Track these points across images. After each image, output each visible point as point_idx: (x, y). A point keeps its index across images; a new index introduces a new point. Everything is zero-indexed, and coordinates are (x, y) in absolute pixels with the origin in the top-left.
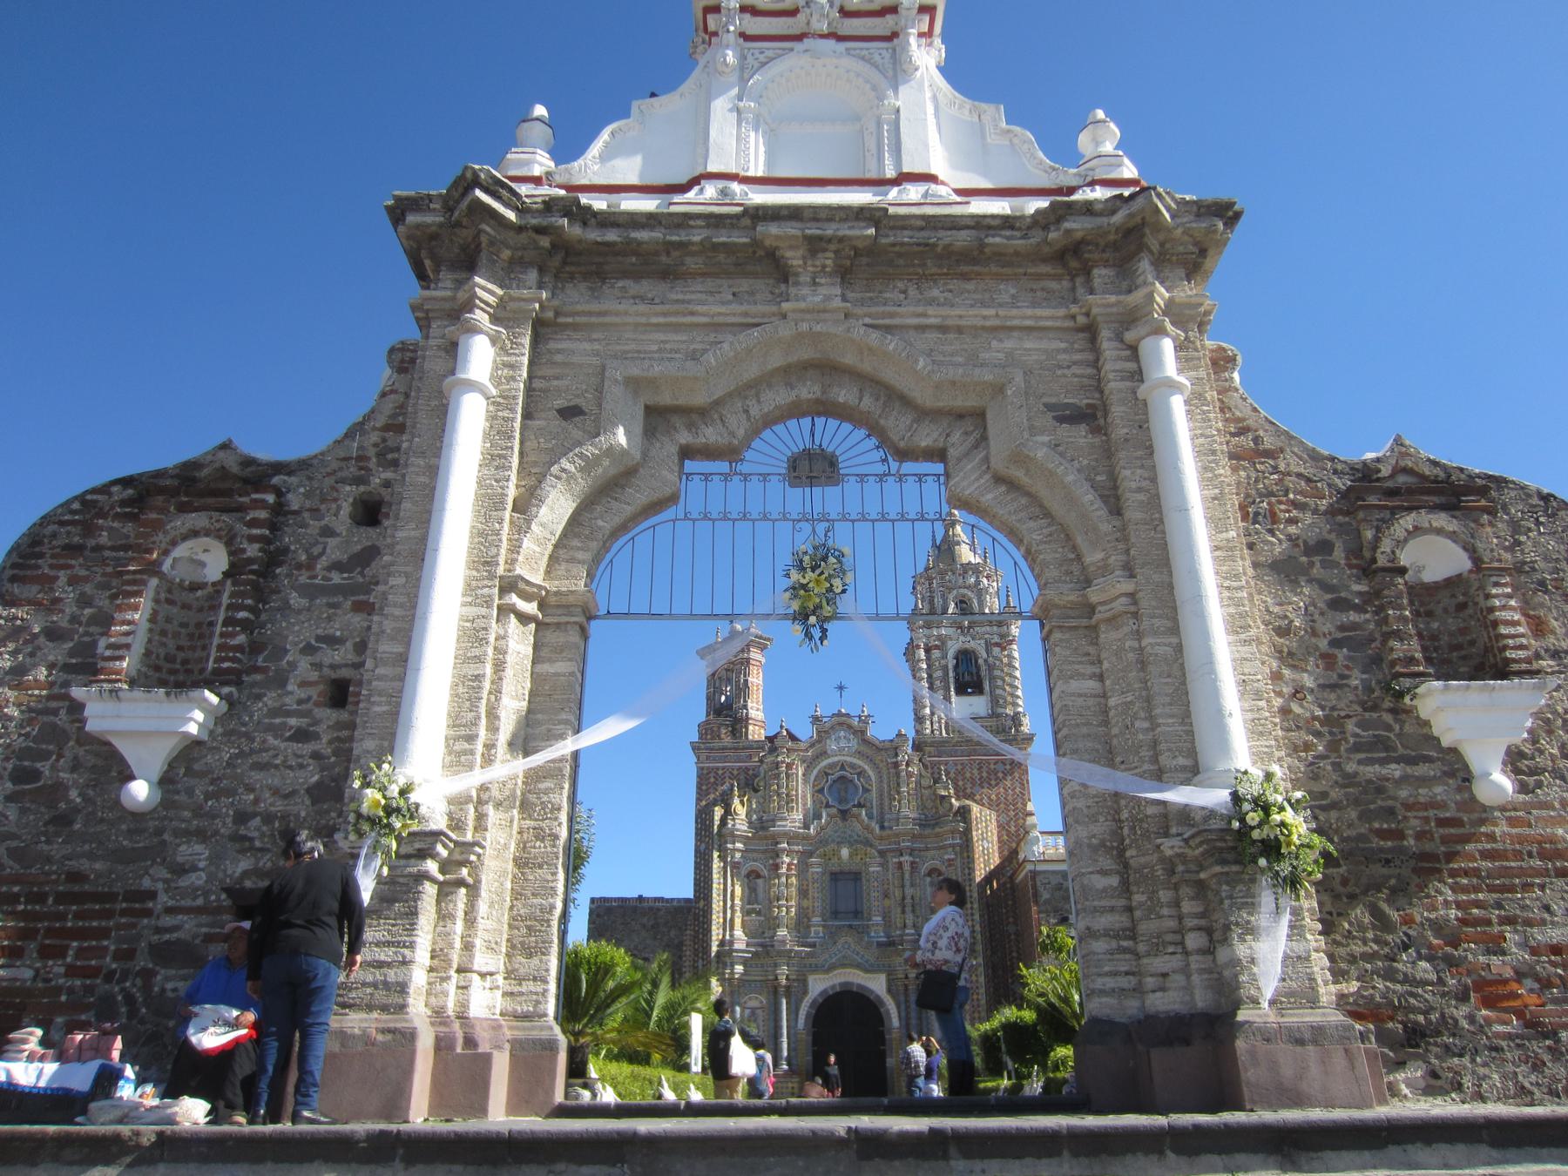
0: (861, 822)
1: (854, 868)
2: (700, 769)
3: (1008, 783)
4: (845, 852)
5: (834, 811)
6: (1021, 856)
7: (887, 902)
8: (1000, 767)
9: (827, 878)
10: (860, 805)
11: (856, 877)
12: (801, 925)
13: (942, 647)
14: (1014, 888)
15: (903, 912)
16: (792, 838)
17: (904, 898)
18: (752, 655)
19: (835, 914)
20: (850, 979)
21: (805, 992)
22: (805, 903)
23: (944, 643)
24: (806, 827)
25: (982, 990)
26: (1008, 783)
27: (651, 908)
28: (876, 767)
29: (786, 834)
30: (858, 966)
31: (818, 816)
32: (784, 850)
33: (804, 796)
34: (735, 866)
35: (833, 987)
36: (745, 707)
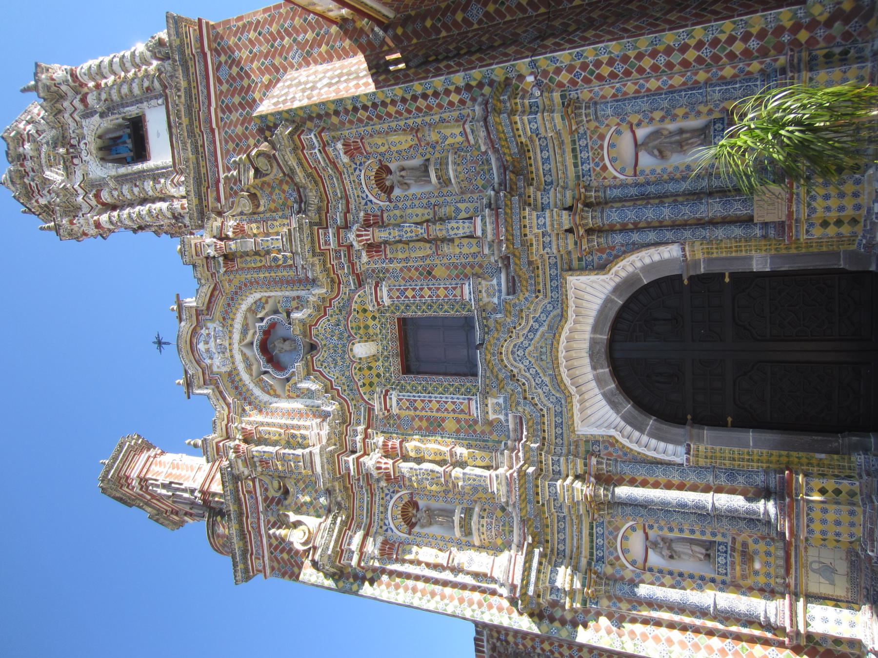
1: (393, 331)
3: (245, 54)
4: (362, 350)
8: (224, 72)
9: (410, 380)
12: (486, 439)
13: (95, 187)
14: (405, 21)
16: (342, 444)
18: (134, 474)
20: (586, 345)
21: (611, 442)
22: (450, 425)
24: (325, 416)
25: (589, 52)
29: (331, 459)
30: (555, 330)
31: (310, 394)
32: (358, 464)
33: (289, 414)
34: (390, 549)
35: (599, 380)
36: (192, 491)
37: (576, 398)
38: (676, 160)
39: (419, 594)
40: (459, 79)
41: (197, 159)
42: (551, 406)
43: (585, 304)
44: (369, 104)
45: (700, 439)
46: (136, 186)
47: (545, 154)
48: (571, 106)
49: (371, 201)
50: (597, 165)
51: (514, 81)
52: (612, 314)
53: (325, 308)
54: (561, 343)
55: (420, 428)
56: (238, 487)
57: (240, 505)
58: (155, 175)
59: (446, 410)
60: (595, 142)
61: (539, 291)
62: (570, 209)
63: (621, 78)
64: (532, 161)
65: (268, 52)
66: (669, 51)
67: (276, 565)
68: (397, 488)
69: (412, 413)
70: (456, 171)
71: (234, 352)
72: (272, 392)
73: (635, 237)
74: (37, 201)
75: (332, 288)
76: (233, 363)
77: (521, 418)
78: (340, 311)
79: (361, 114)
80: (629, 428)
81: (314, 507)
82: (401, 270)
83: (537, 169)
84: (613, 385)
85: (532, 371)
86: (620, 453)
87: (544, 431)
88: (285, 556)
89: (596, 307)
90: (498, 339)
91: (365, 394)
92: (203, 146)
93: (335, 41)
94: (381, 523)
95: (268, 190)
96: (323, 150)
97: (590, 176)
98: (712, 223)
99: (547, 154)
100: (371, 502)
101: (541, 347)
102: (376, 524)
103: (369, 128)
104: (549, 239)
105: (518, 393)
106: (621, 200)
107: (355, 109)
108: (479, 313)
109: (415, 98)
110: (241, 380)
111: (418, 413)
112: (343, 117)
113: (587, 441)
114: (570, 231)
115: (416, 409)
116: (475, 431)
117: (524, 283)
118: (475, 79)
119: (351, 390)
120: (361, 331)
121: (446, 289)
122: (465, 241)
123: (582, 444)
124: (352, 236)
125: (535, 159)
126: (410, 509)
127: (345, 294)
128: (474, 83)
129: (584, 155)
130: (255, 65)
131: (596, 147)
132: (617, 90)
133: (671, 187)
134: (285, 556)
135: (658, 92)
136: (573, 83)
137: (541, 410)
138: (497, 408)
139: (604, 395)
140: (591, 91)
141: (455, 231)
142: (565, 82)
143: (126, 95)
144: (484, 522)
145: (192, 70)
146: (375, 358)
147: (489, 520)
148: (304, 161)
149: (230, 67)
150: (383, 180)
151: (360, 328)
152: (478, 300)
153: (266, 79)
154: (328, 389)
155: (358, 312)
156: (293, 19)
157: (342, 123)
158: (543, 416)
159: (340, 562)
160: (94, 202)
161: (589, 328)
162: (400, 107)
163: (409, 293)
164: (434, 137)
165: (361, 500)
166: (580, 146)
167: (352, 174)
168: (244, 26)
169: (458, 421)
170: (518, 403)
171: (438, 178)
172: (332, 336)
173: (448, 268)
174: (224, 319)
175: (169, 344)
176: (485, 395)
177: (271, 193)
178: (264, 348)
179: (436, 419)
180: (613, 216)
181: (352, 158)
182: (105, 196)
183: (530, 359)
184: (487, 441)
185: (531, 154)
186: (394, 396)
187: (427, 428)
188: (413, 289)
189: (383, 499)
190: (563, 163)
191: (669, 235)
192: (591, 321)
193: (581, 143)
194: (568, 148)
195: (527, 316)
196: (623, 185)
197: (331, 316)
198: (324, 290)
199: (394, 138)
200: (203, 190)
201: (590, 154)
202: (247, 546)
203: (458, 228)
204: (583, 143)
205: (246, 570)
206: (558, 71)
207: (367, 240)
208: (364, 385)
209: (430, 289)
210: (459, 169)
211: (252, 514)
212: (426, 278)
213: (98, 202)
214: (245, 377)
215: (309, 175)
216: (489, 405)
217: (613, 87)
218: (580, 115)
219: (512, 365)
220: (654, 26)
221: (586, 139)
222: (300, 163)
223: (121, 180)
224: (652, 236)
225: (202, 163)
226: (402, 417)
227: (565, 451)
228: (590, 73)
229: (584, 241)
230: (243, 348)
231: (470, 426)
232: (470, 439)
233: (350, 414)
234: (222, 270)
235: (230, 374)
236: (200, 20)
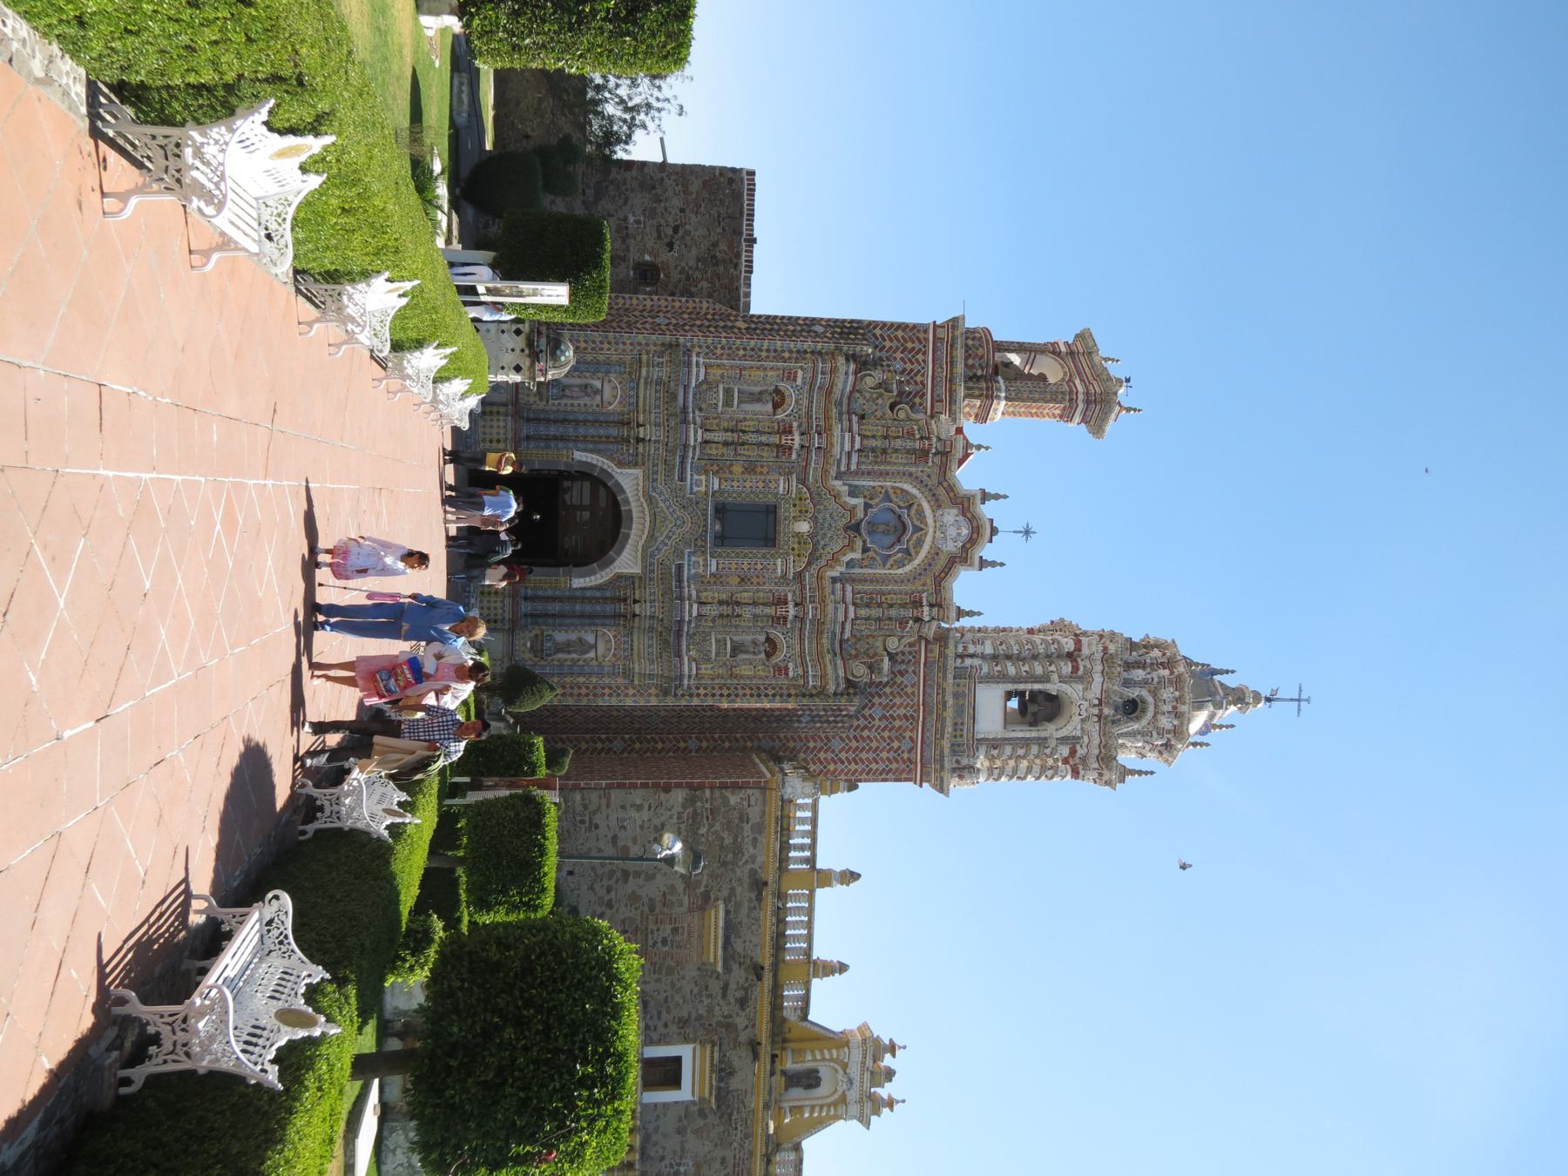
0: (842, 551)
1: (781, 538)
2: (923, 329)
4: (804, 527)
5: (860, 514)
6: (787, 767)
8: (906, 745)
9: (771, 499)
10: (865, 550)
13: (1074, 677)
15: (721, 603)
17: (738, 604)
19: (721, 510)
21: (620, 464)
23: (1080, 679)
25: (614, 702)
26: (884, 755)
27: (738, 255)
28: (916, 576)
30: (652, 536)
35: (627, 502)
38: (573, 636)
40: (696, 702)
45: (566, 464)
48: (628, 674)
52: (617, 545)
58: (1003, 678)
62: (635, 615)
66: (572, 695)
67: (921, 336)
73: (598, 594)
79: (770, 692)
88: (909, 345)
95: (871, 652)
98: (554, 599)
100: (810, 407)
106: (606, 617)
107: (774, 695)
113: (636, 465)
114: (635, 602)
124: (792, 611)
130: (874, 744)
133: (577, 621)
134: (909, 345)
135: (579, 675)
150: (772, 646)
153: (866, 733)
154: (837, 497)
160: (1081, 665)
162: (741, 692)
163: (759, 567)
165: (818, 407)
176: (706, 493)
180: (609, 608)
182: (1067, 668)
191: (578, 594)
196: (604, 625)
205: (953, 327)
214: (925, 505)
220: (579, 710)
223: (1045, 679)
224: (588, 594)
228: (615, 691)
235: (939, 507)
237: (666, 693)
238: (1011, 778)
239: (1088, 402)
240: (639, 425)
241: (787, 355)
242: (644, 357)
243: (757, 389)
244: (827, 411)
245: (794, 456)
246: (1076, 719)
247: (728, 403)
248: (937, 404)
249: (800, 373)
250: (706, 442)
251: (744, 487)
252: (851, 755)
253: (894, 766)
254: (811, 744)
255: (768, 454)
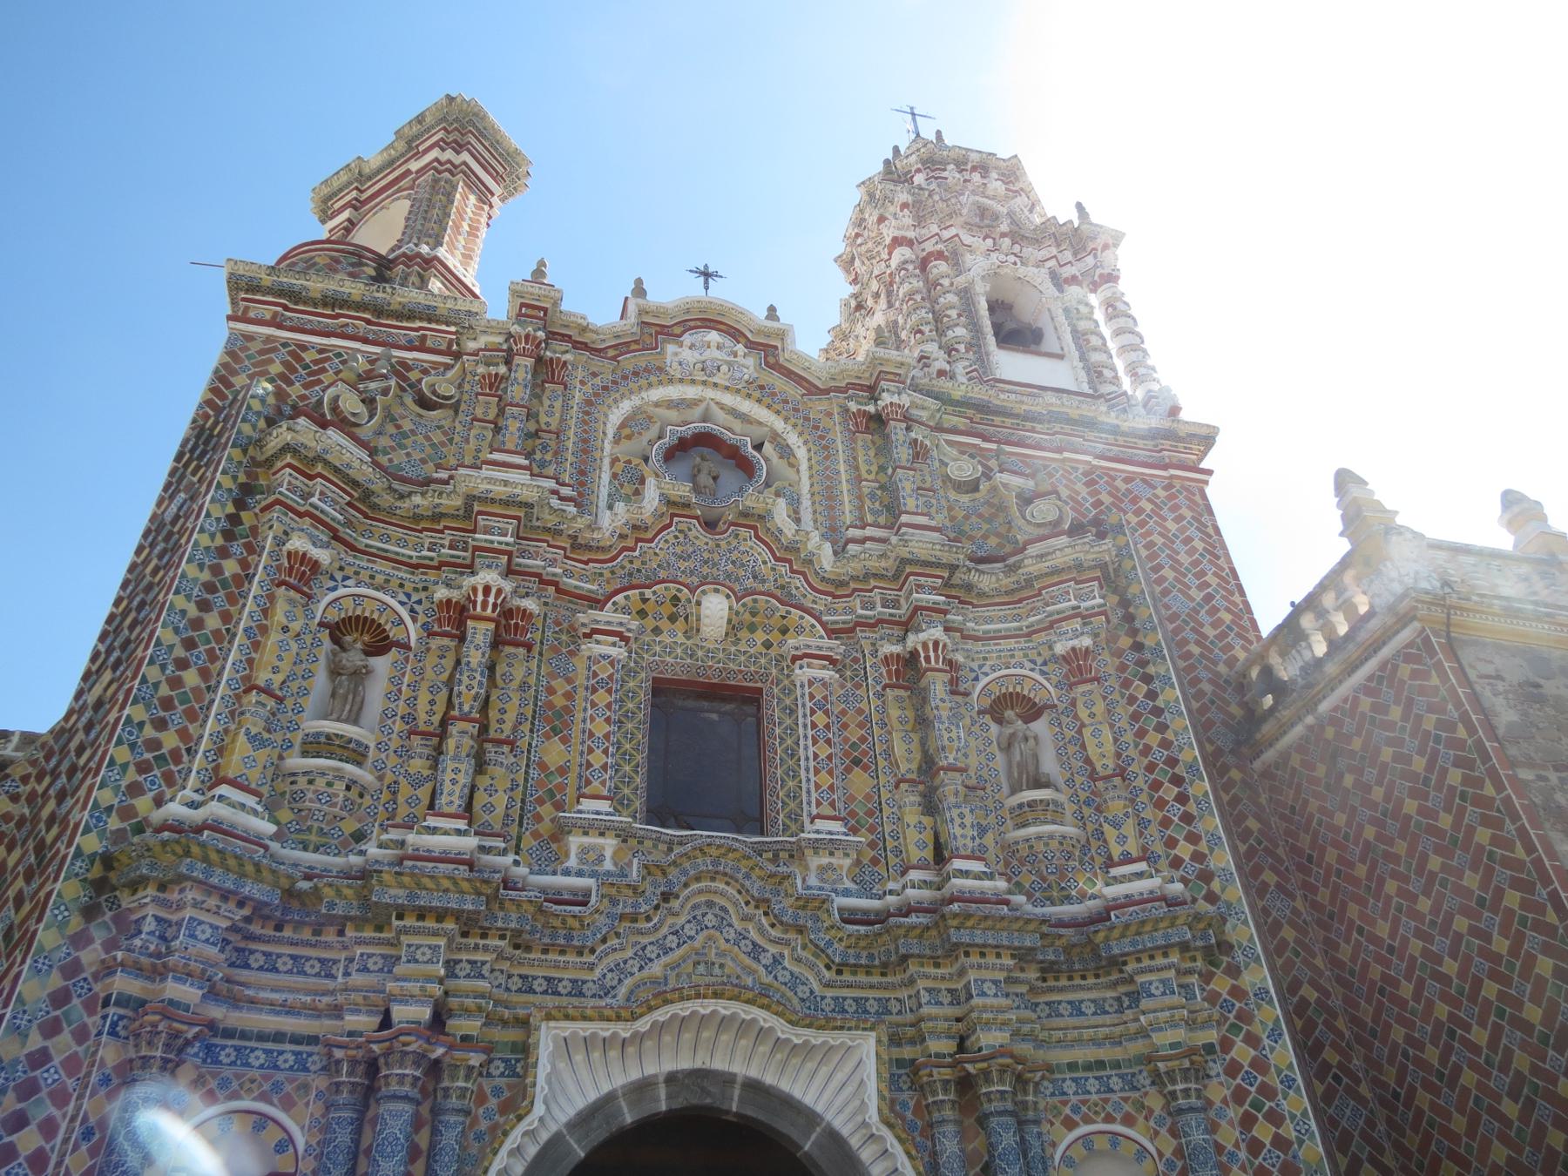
4: (715, 609)
7: (860, 781)
11: (744, 699)
13: (954, 258)
20: (719, 1064)
21: (516, 1103)
25: (1297, 1103)
26: (1172, 527)
35: (642, 1088)
37: (624, 1030)
39: (193, 612)
40: (1223, 859)
41: (1017, 416)
42: (597, 973)
43: (810, 1066)
44: (1160, 703)
46: (959, 315)
47: (1089, 1009)
48: (1196, 1062)
49: (976, 679)
50: (1076, 1109)
51: (1225, 959)
52: (783, 1126)
53: (789, 561)
54: (747, 1007)
55: (551, 691)
56: (438, 322)
57: (399, 316)
59: (591, 751)
60: (1117, 1107)
61: (839, 972)
63: (1252, 1164)
64: (1077, 981)
65: (1177, 561)
67: (255, 347)
68: (421, 618)
69: (581, 680)
70: (1051, 837)
71: (700, 388)
72: (627, 431)
74: (918, 171)
75: (823, 579)
76: (681, 381)
77: (584, 904)
78: (782, 587)
80: (532, 1151)
81: (392, 448)
82: (860, 711)
83: (1061, 990)
84: (629, 1119)
85: (672, 941)
86: (484, 1125)
87: (545, 951)
89: (797, 1093)
90: (747, 876)
91: (627, 598)
92: (1033, 430)
93: (1206, 668)
94: (349, 571)
96: (1076, 613)
97: (1053, 1094)
99: (1089, 1012)
101: (722, 966)
102: (351, 560)
103: (1116, 696)
104: (946, 1001)
105: (635, 905)
107: (1148, 679)
108: (788, 846)
109: (1177, 780)
110: (650, 385)
111: (581, 693)
112: (1132, 656)
115: (594, 690)
116: (541, 802)
117: (863, 943)
118: (1223, 890)
119: (631, 575)
120: (747, 616)
121: (831, 787)
122: (928, 837)
123: (513, 1035)
125: (1082, 988)
126: (366, 638)
127: (815, 602)
128: (1216, 885)
129: (1092, 1085)
130: (1160, 541)
131: (1109, 1108)
132: (1232, 1155)
136: (1233, 1069)
137: (592, 951)
138: (592, 856)
139: (610, 1098)
140: (1225, 1101)
141: (958, 821)
142: (1233, 1054)
143: (1088, 341)
144: (340, 787)
145: (1141, 443)
146: (693, 630)
147: (340, 799)
148: (1056, 579)
149: (1149, 500)
150: (1013, 706)
151: (754, 614)
152: (816, 846)
155: (784, 617)
156: (1228, 610)
157: (1118, 653)
158: (580, 954)
159: (289, 465)
161: (753, 1073)
162: (1160, 755)
164: (1116, 807)
166: (1109, 1077)
167: (1026, 656)
168: (1210, 537)
169: (562, 771)
170: (614, 902)
171: (1032, 804)
172: (733, 562)
173: (868, 797)
174: (762, 387)
175: (707, 288)
176: (624, 835)
177: (980, 516)
178: (705, 440)
179: (567, 725)
181: (1065, 659)
183: (701, 938)
184: (521, 825)
185: (1091, 981)
186: (618, 652)
187: (550, 705)
188: (827, 726)
189: (401, 585)
190: (1079, 1041)
192: (769, 1079)
193: (1115, 1079)
194: (1105, 1053)
195: (787, 943)
197: (773, 569)
198: (828, 568)
199: (1108, 736)
200: (970, 412)
201: (1095, 1097)
202: (305, 303)
203: (963, 826)
204: (1116, 1083)
205: (253, 287)
206: (1252, 1040)
207: (928, 659)
208: (645, 601)
209: (830, 757)
210: (1054, 844)
211: (375, 333)
212: (847, 754)
213: (930, 254)
215: (1029, 583)
216: (601, 840)
217: (1237, 1145)
218: (1186, 1079)
219: (687, 899)
221: (1122, 1090)
222: (1056, 571)
223: (966, 294)
225: (1009, 422)
226: (574, 660)
227: (500, 994)
228: (1256, 1103)
229: (946, 1073)
230: (703, 406)
231: (551, 794)
232: (525, 788)
233: (586, 563)
234: (853, 406)
236: (1210, 472)
237: (1218, 952)
238: (1144, 351)
239: (459, 147)
240: (386, 1023)
241: (230, 567)
242: (123, 983)
243: (321, 682)
244: (416, 521)
245: (530, 604)
246: (1022, 271)
247: (356, 754)
248: (429, 343)
249: (297, 543)
250: (468, 810)
251: (601, 752)
252: (1190, 578)
253: (1188, 514)
254: (1196, 650)
255: (517, 667)
